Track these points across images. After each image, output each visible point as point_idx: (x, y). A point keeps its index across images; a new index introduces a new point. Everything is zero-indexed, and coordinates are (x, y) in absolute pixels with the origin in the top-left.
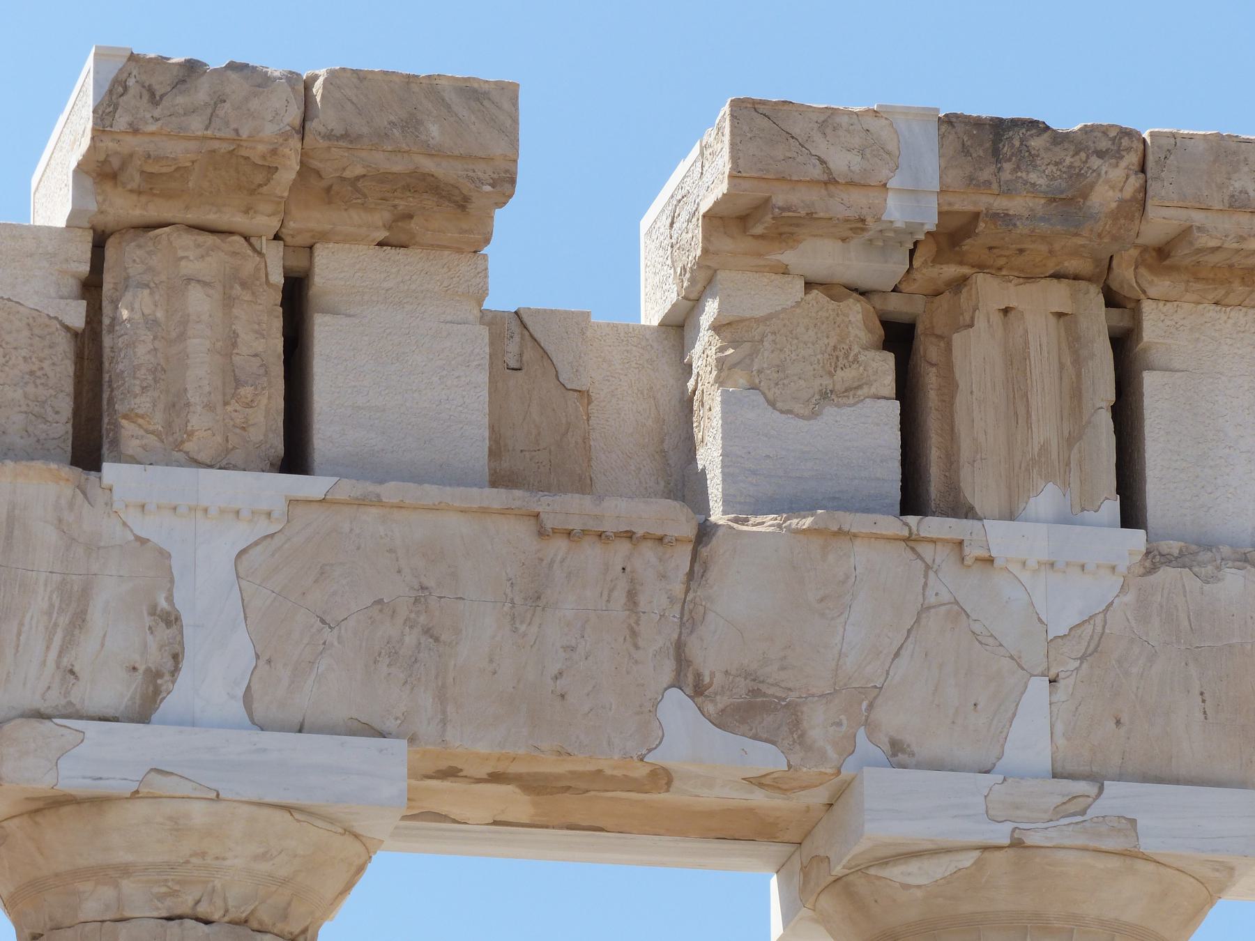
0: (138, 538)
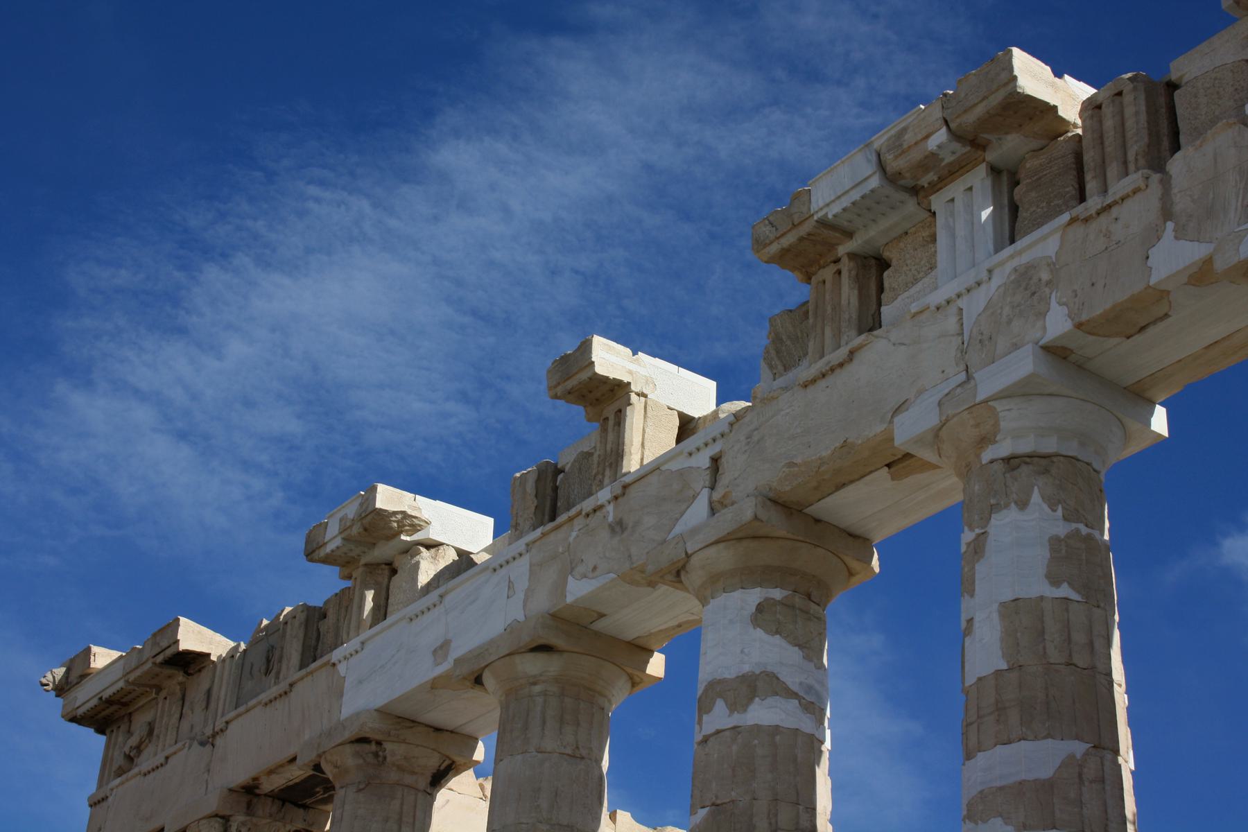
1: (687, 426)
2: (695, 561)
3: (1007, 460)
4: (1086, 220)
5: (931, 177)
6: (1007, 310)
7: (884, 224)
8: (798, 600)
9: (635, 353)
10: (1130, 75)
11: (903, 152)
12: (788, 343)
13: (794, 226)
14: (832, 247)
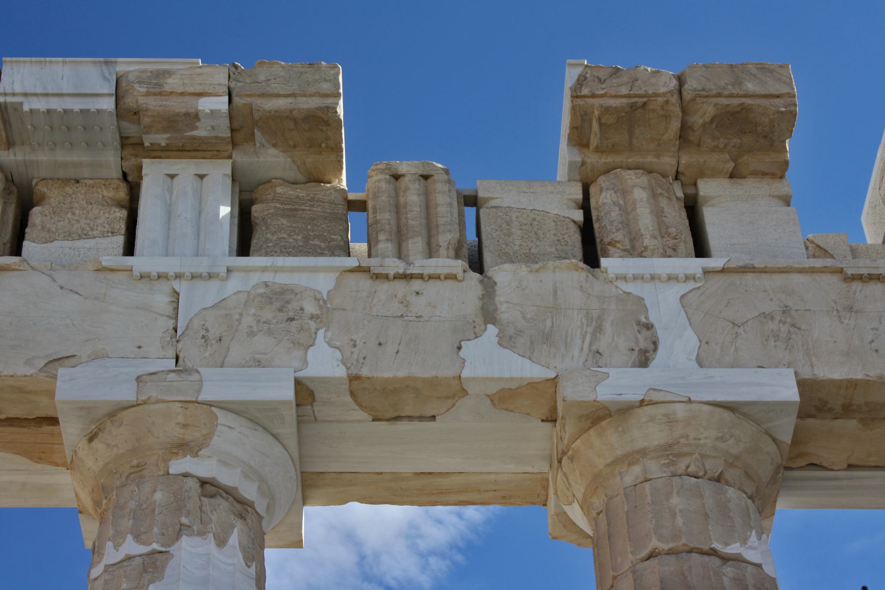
0: (625, 292)
4: (377, 277)
5: (161, 139)
6: (248, 321)
7: (61, 156)
10: (440, 166)
11: (160, 94)
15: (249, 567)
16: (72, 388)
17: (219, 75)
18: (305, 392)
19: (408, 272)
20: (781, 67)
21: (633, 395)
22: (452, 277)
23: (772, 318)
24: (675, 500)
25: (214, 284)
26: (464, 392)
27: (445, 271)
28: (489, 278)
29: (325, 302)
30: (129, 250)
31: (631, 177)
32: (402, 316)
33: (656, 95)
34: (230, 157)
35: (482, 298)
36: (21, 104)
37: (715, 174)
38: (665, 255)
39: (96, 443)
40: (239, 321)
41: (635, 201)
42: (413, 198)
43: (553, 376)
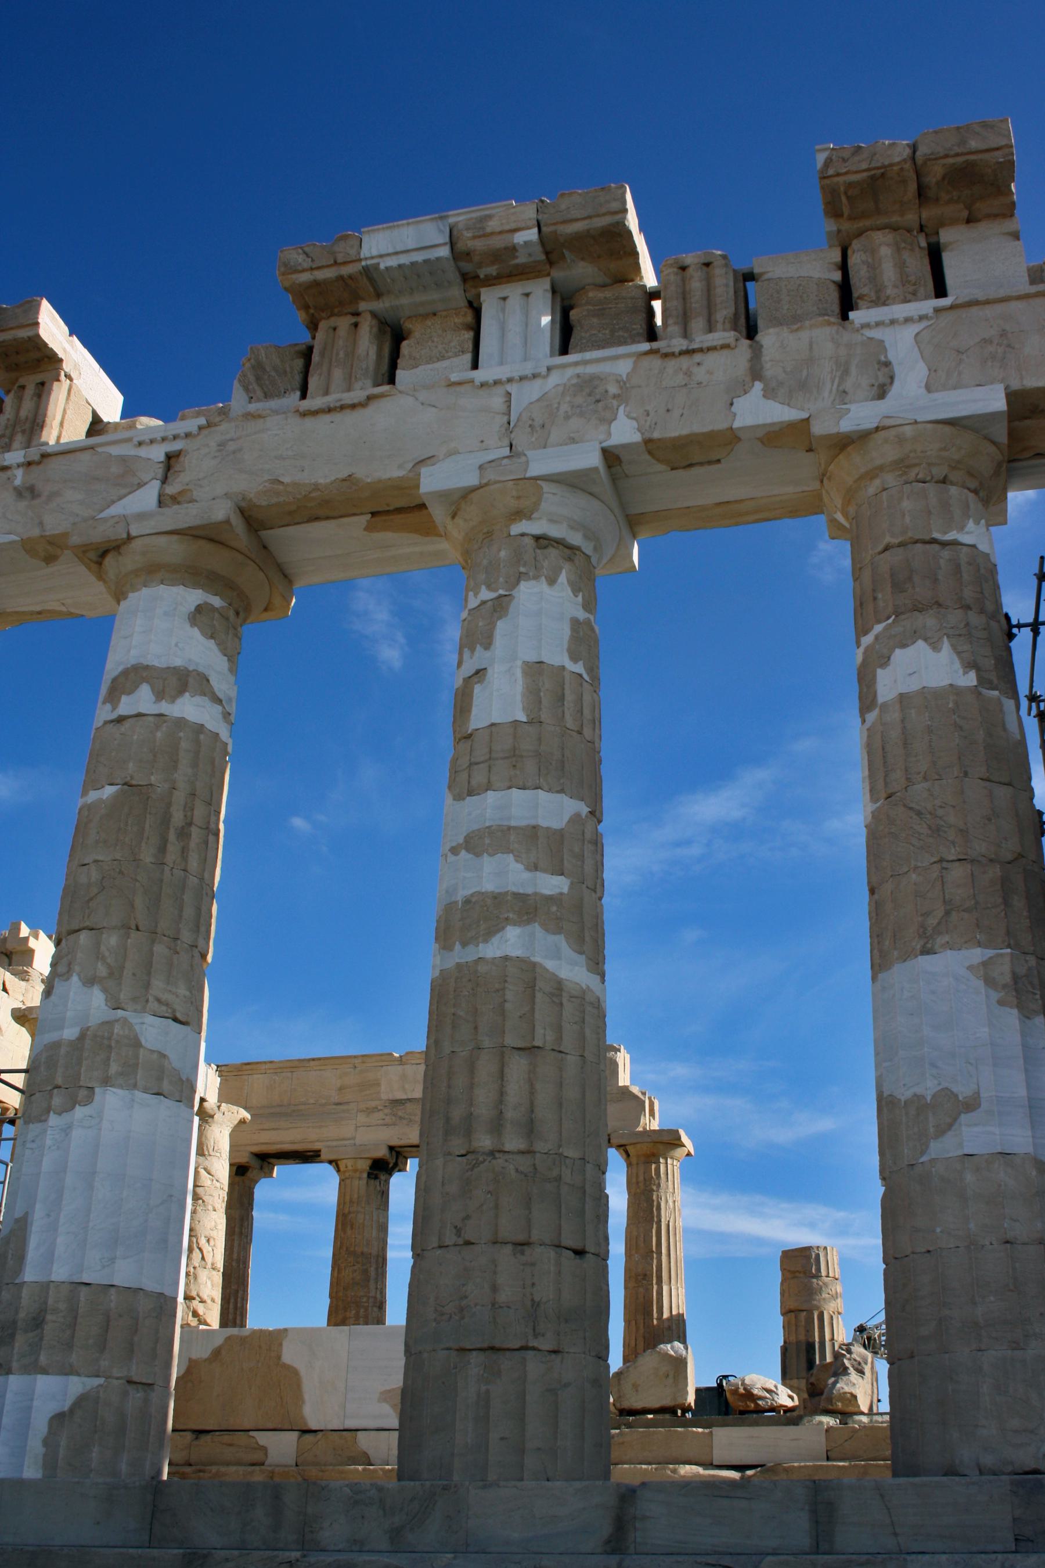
0: (869, 338)
1: (96, 426)
2: (136, 544)
3: (537, 538)
4: (666, 355)
5: (492, 270)
6: (565, 407)
7: (419, 298)
8: (231, 614)
9: (71, 335)
10: (719, 252)
11: (484, 235)
12: (273, 374)
13: (336, 263)
14: (356, 297)
15: (577, 596)
16: (433, 481)
17: (529, 212)
18: (611, 457)
19: (690, 348)
20: (1002, 121)
21: (869, 424)
22: (726, 346)
23: (991, 342)
24: (906, 504)
25: (538, 382)
26: (739, 439)
27: (721, 342)
28: (757, 342)
29: (625, 383)
30: (475, 366)
31: (879, 237)
32: (686, 385)
33: (891, 165)
34: (549, 275)
35: (751, 360)
36: (378, 264)
37: (953, 222)
38: (906, 301)
39: (457, 520)
40: (558, 409)
41: (883, 256)
42: (696, 285)
43: (807, 416)
